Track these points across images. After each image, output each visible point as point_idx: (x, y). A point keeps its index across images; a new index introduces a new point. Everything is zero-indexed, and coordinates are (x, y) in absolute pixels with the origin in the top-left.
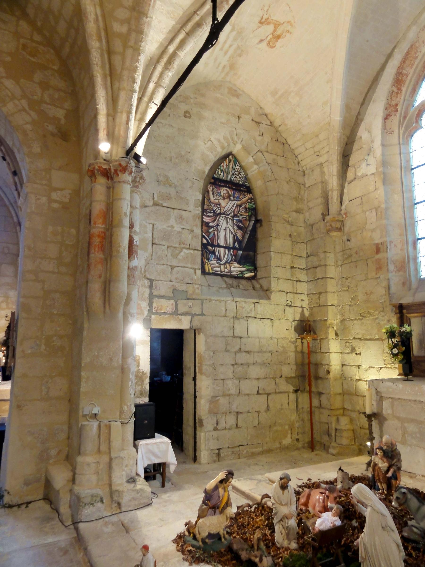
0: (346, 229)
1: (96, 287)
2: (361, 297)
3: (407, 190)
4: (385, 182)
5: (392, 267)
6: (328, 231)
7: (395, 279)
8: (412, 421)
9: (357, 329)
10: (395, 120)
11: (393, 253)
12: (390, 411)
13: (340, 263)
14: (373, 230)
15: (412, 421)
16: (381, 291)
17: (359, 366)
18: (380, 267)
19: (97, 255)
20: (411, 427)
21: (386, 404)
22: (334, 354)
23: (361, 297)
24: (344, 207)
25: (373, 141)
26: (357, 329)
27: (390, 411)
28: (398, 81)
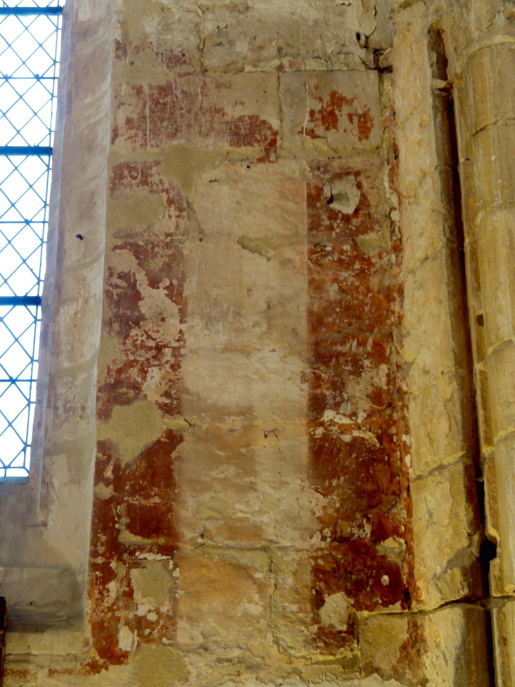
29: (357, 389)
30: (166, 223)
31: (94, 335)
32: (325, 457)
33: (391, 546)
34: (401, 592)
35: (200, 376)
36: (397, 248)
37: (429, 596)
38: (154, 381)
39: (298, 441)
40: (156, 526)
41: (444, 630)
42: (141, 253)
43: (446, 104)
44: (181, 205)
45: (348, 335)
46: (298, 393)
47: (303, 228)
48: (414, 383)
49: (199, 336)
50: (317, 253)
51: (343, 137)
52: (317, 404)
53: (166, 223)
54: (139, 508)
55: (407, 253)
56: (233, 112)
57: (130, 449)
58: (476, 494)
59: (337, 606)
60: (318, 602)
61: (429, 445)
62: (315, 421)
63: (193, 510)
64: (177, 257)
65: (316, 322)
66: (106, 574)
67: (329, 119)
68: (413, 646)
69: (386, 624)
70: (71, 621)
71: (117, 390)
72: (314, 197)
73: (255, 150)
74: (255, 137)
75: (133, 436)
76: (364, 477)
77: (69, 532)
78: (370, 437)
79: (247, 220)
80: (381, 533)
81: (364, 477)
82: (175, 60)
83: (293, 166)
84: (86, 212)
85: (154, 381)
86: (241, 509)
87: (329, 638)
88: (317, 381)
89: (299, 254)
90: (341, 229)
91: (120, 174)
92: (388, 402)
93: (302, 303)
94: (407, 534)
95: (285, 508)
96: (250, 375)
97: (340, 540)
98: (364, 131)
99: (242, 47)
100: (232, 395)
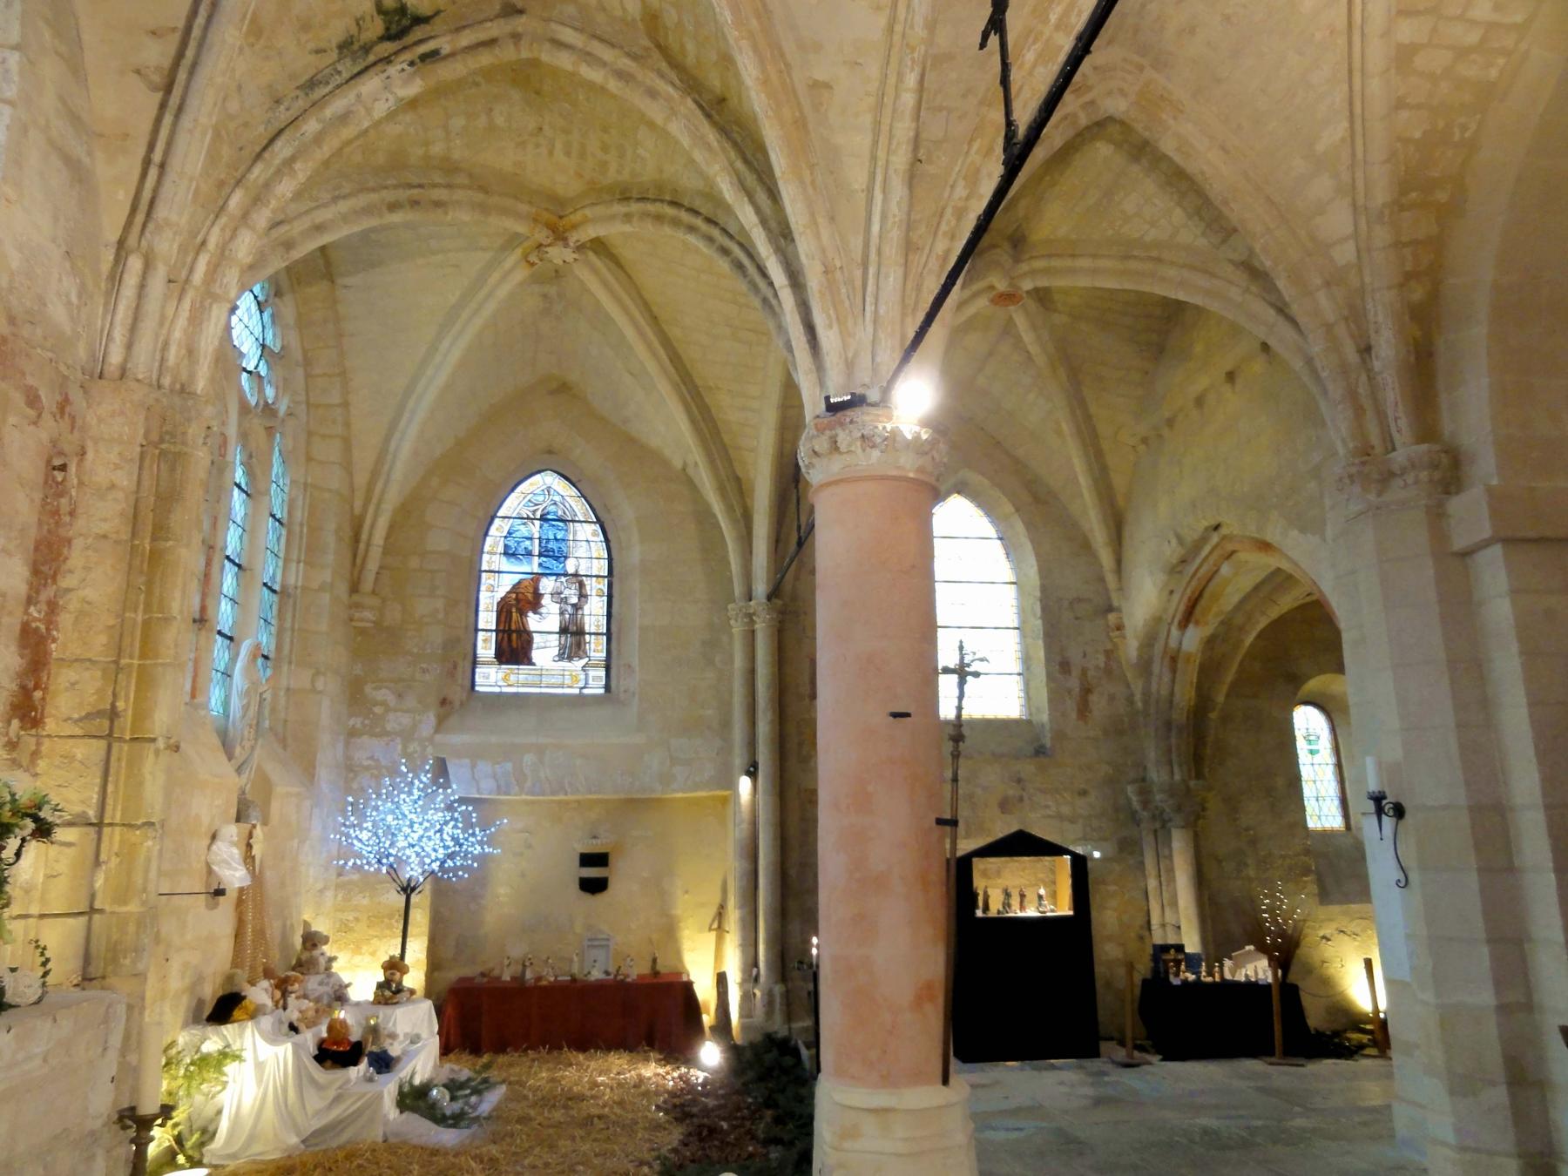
33: (38, 694)
36: (72, 514)
46: (23, 589)
47: (41, 480)
48: (72, 603)
52: (30, 601)
55: (80, 523)
56: (30, 381)
60: (9, 723)
62: (26, 612)
68: (35, 755)
73: (32, 413)
78: (43, 627)
80: (37, 687)
88: (31, 585)
89: (38, 496)
92: (53, 607)
93: (33, 533)
94: (45, 690)
97: (23, 687)
99: (39, 332)
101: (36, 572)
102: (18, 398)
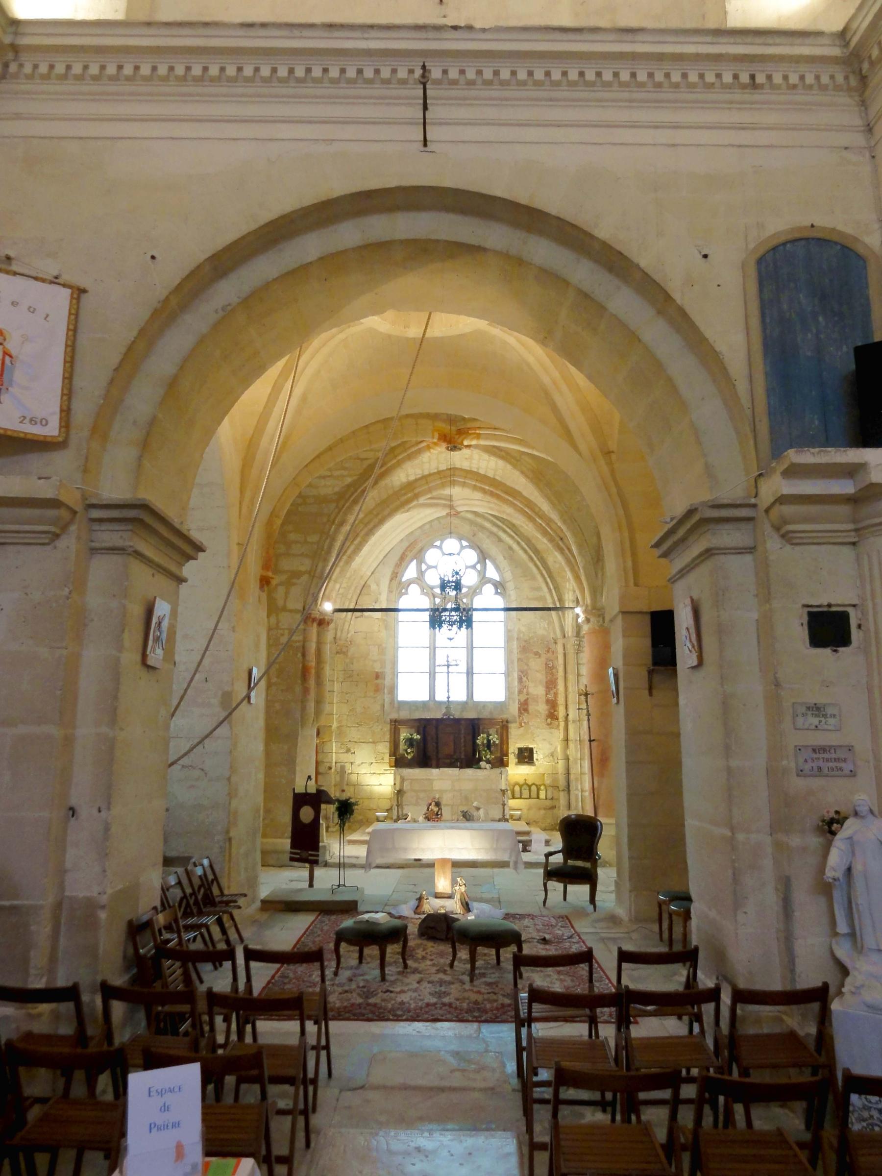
0: (350, 654)
1: (311, 706)
2: (359, 709)
3: (394, 636)
4: (386, 627)
5: (386, 691)
6: (337, 653)
7: (387, 700)
8: (425, 791)
9: (353, 734)
10: (395, 583)
11: (387, 682)
12: (409, 787)
13: (341, 680)
14: (375, 661)
15: (425, 791)
16: (378, 707)
17: (352, 763)
18: (378, 689)
19: (312, 683)
20: (422, 795)
21: (405, 783)
22: (335, 754)
23: (359, 709)
24: (349, 635)
25: (380, 594)
26: (353, 734)
27: (409, 787)
28: (402, 558)
29: (552, 692)
30: (526, 668)
31: (516, 683)
32: (548, 701)
34: (557, 719)
35: (531, 690)
37: (560, 720)
38: (525, 691)
39: (544, 699)
40: (526, 710)
41: (562, 724)
42: (522, 672)
43: (565, 654)
44: (528, 665)
45: (550, 685)
46: (544, 693)
49: (531, 684)
50: (546, 673)
51: (550, 655)
53: (526, 668)
54: (524, 707)
57: (522, 700)
58: (567, 708)
59: (549, 720)
61: (561, 700)
63: (531, 708)
64: (527, 674)
65: (547, 682)
66: (520, 717)
67: (548, 652)
68: (558, 726)
69: (556, 722)
70: (516, 722)
71: (520, 692)
72: (546, 664)
74: (537, 654)
75: (523, 698)
76: (552, 704)
77: (514, 709)
79: (536, 665)
81: (552, 704)
82: (526, 641)
83: (543, 659)
84: (512, 662)
85: (525, 691)
86: (537, 708)
87: (548, 724)
89: (544, 672)
90: (550, 669)
91: (519, 660)
92: (556, 694)
93: (545, 680)
95: (542, 708)
96: (538, 690)
98: (553, 652)
100: (535, 693)
101: (547, 687)
102: (531, 655)
